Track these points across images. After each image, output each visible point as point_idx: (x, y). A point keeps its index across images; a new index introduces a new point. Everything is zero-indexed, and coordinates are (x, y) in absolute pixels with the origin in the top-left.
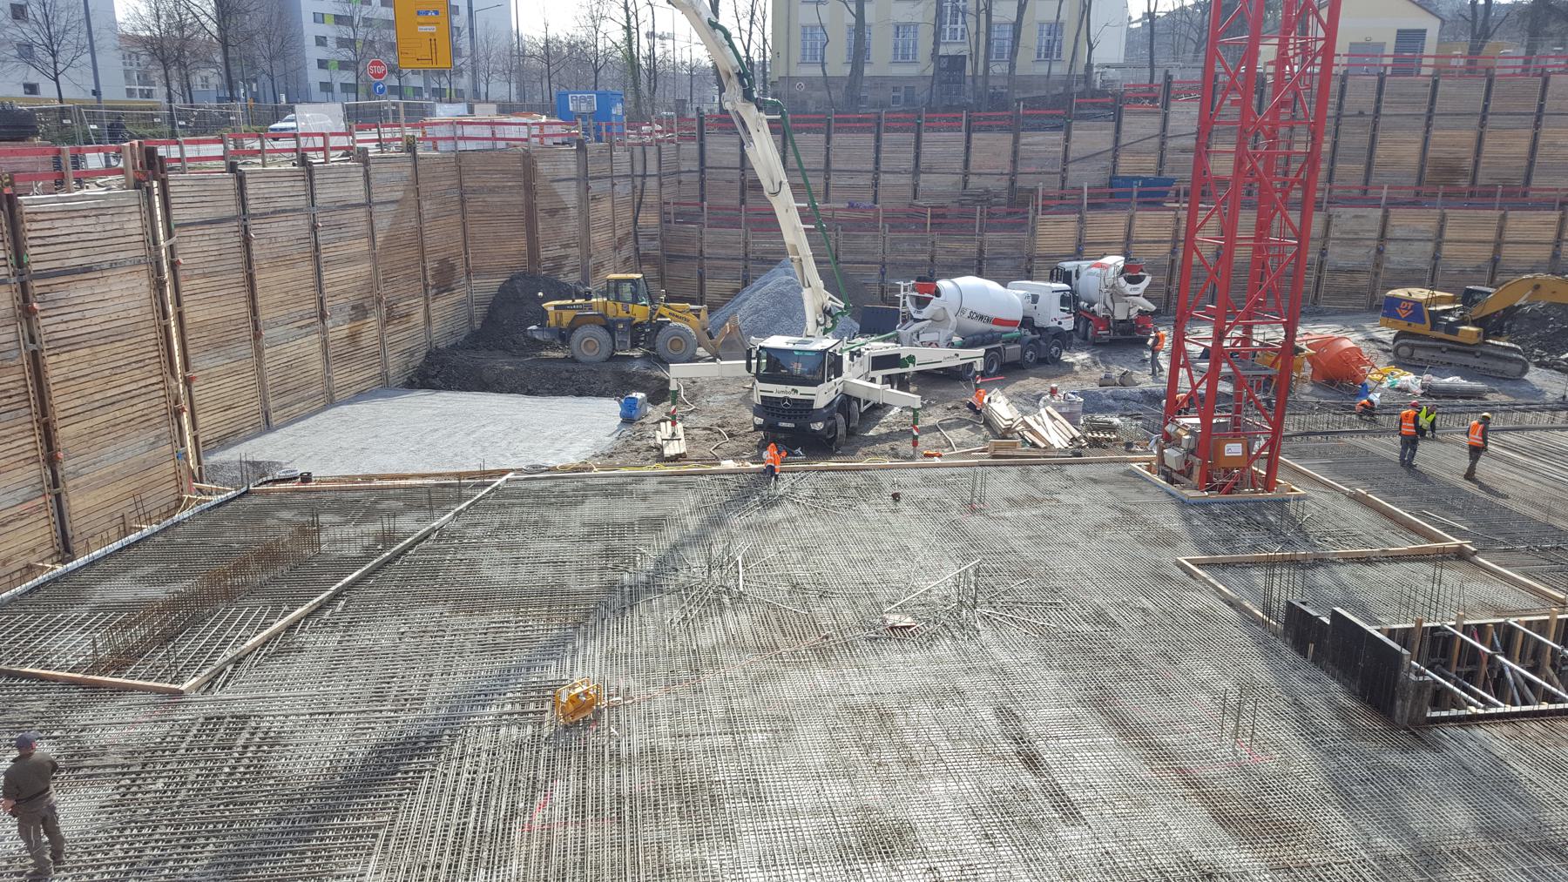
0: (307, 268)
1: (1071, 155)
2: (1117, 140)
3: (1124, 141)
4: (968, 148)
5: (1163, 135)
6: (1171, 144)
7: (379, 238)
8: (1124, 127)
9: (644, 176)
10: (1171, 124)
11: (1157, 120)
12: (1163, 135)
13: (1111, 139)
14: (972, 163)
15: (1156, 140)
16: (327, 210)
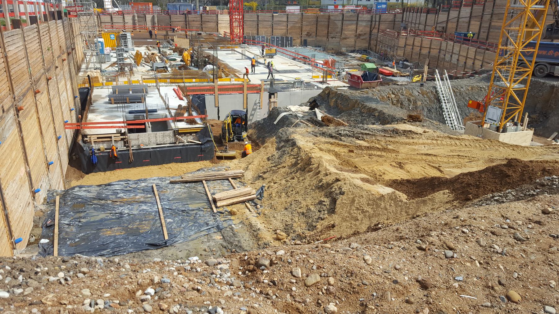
0: (270, 29)
1: (439, 22)
2: (448, 18)
3: (450, 18)
4: (426, 18)
5: (458, 18)
6: (460, 20)
7: (289, 27)
8: (450, 15)
9: (375, 21)
10: (461, 14)
11: (457, 12)
12: (458, 18)
13: (447, 18)
14: (427, 23)
15: (457, 19)
16: (275, 21)
